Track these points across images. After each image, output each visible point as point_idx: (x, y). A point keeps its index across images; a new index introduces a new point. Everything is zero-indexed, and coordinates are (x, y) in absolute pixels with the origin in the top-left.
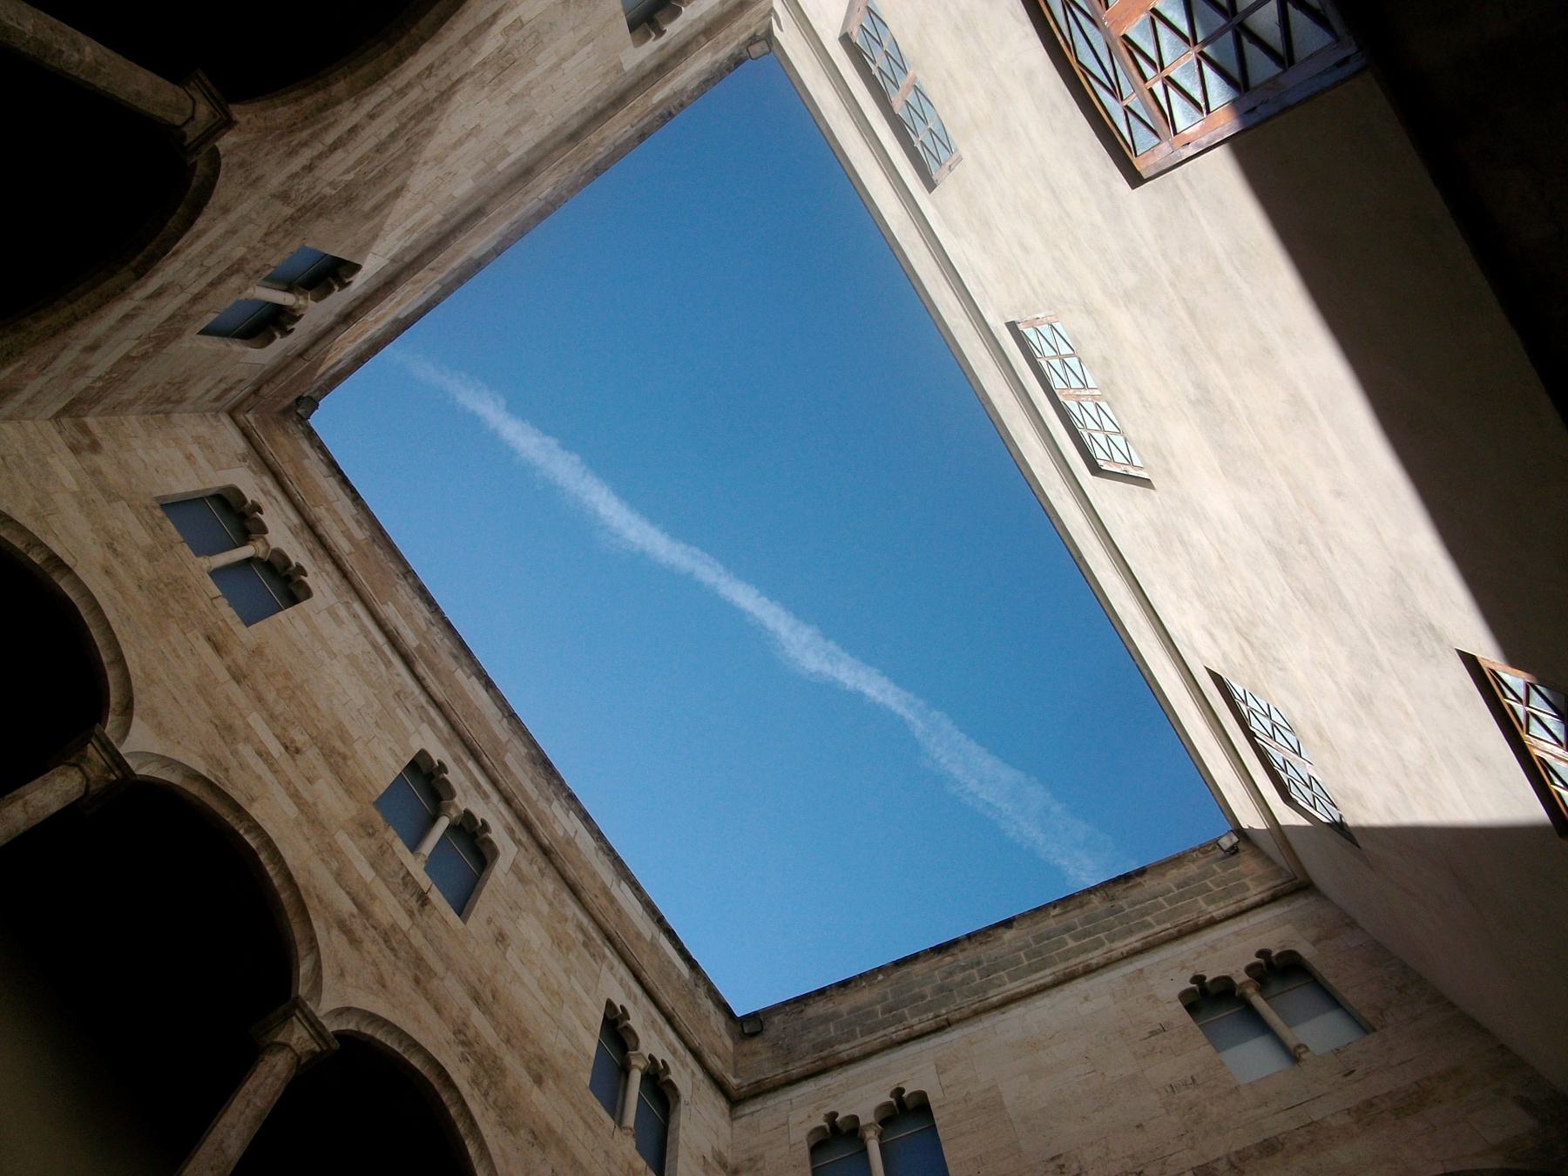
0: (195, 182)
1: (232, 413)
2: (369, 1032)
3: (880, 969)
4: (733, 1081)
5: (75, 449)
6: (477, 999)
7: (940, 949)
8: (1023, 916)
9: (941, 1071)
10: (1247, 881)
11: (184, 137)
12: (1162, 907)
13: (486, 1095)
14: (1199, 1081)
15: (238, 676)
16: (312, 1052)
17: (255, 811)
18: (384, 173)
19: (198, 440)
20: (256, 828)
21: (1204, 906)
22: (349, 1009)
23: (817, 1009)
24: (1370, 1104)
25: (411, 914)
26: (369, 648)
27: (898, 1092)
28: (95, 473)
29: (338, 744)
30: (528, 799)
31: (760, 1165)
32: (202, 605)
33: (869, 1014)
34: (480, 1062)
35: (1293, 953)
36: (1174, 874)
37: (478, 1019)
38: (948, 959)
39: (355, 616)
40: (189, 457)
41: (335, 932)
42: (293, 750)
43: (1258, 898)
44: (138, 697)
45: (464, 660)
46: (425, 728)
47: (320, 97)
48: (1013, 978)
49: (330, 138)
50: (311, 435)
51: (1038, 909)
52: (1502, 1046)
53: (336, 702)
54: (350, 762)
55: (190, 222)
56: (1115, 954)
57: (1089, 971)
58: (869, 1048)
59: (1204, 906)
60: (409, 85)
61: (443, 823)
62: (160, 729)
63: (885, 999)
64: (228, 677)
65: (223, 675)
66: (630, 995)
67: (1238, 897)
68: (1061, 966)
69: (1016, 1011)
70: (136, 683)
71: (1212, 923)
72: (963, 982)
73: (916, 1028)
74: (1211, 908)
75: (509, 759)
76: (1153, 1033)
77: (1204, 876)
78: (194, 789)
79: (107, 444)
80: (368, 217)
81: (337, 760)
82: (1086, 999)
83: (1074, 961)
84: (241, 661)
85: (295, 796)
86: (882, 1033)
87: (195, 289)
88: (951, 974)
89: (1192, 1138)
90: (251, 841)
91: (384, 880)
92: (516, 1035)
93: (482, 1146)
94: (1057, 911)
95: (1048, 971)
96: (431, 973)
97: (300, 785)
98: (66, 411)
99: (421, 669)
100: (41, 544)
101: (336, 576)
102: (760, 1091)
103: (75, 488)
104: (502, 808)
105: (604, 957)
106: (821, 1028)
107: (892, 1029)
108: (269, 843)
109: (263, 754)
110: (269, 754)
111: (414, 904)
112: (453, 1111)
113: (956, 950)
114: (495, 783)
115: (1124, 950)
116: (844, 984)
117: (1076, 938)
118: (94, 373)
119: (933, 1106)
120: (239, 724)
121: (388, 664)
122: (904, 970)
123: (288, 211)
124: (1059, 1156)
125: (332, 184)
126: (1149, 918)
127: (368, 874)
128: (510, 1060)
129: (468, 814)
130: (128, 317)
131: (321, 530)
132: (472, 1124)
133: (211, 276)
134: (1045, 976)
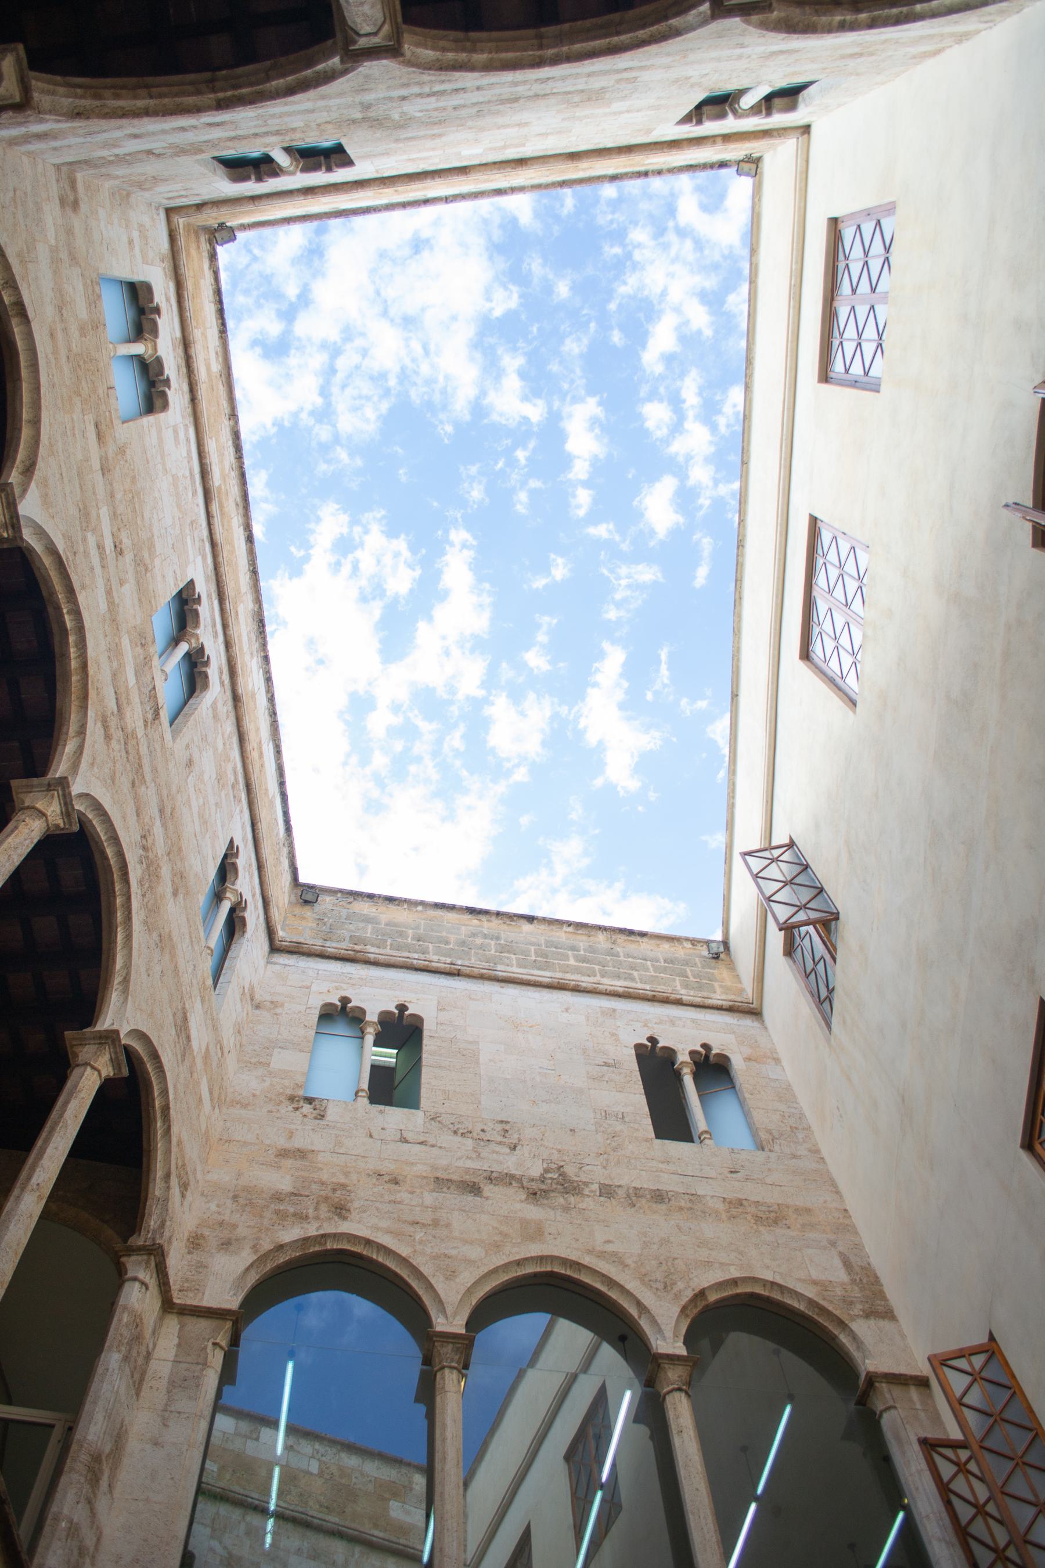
0: (320, 67)
1: (169, 211)
2: (90, 816)
3: (422, 903)
4: (281, 934)
5: (63, 202)
6: (161, 811)
7: (472, 911)
9: (441, 1009)
10: (716, 984)
11: (355, 42)
12: (647, 970)
13: (144, 896)
14: (627, 1119)
15: (105, 470)
16: (57, 826)
17: (81, 598)
18: (440, 122)
19: (141, 227)
20: (77, 613)
21: (679, 988)
22: (87, 795)
23: (363, 908)
24: (740, 1203)
25: (145, 721)
26: (188, 474)
27: (402, 1008)
28: (70, 232)
29: (146, 555)
30: (241, 649)
31: (279, 1011)
32: (100, 391)
33: (401, 934)
34: (148, 867)
35: (726, 1058)
36: (666, 946)
37: (158, 830)
38: (475, 922)
39: (188, 440)
40: (131, 242)
41: (99, 724)
42: (119, 551)
43: (720, 1003)
44: (40, 464)
45: (241, 510)
46: (199, 559)
47: (463, 56)
48: (519, 966)
49: (437, 88)
50: (213, 257)
51: (557, 921)
52: (846, 1210)
53: (155, 516)
54: (148, 574)
55: (291, 91)
57: (576, 989)
58: (393, 960)
59: (679, 988)
60: (525, 82)
61: (184, 648)
62: (46, 501)
63: (417, 927)
64: (98, 467)
65: (96, 465)
66: (244, 839)
67: (705, 994)
68: (559, 975)
69: (512, 991)
70: (42, 451)
71: (679, 1003)
72: (482, 947)
73: (434, 964)
74: (683, 992)
75: (241, 609)
76: (606, 1064)
77: (686, 963)
78: (47, 561)
79: (84, 207)
80: (397, 140)
81: (142, 567)
82: (567, 1010)
83: (568, 976)
84: (110, 454)
85: (109, 592)
87: (240, 133)
88: (474, 935)
89: (607, 1160)
90: (69, 622)
91: (139, 689)
92: (175, 851)
93: (129, 937)
94: (570, 929)
95: (548, 974)
96: (143, 781)
97: (114, 582)
98: (70, 164)
99: (215, 508)
100: (15, 288)
101: (187, 397)
102: (297, 950)
103: (53, 242)
104: (222, 648)
105: (240, 801)
106: (361, 925)
108: (81, 629)
109: (100, 547)
110: (104, 548)
111: (150, 716)
112: (119, 901)
113: (484, 918)
114: (225, 626)
116: (390, 900)
117: (578, 959)
118: (117, 151)
119: (426, 1033)
120: (94, 514)
121: (195, 493)
122: (439, 913)
123: (359, 116)
124: (507, 1122)
125: (403, 114)
126: (635, 974)
127: (132, 681)
128: (165, 872)
129: (201, 650)
130: (183, 129)
131: (192, 352)
132: (128, 918)
133: (264, 130)
134: (545, 975)
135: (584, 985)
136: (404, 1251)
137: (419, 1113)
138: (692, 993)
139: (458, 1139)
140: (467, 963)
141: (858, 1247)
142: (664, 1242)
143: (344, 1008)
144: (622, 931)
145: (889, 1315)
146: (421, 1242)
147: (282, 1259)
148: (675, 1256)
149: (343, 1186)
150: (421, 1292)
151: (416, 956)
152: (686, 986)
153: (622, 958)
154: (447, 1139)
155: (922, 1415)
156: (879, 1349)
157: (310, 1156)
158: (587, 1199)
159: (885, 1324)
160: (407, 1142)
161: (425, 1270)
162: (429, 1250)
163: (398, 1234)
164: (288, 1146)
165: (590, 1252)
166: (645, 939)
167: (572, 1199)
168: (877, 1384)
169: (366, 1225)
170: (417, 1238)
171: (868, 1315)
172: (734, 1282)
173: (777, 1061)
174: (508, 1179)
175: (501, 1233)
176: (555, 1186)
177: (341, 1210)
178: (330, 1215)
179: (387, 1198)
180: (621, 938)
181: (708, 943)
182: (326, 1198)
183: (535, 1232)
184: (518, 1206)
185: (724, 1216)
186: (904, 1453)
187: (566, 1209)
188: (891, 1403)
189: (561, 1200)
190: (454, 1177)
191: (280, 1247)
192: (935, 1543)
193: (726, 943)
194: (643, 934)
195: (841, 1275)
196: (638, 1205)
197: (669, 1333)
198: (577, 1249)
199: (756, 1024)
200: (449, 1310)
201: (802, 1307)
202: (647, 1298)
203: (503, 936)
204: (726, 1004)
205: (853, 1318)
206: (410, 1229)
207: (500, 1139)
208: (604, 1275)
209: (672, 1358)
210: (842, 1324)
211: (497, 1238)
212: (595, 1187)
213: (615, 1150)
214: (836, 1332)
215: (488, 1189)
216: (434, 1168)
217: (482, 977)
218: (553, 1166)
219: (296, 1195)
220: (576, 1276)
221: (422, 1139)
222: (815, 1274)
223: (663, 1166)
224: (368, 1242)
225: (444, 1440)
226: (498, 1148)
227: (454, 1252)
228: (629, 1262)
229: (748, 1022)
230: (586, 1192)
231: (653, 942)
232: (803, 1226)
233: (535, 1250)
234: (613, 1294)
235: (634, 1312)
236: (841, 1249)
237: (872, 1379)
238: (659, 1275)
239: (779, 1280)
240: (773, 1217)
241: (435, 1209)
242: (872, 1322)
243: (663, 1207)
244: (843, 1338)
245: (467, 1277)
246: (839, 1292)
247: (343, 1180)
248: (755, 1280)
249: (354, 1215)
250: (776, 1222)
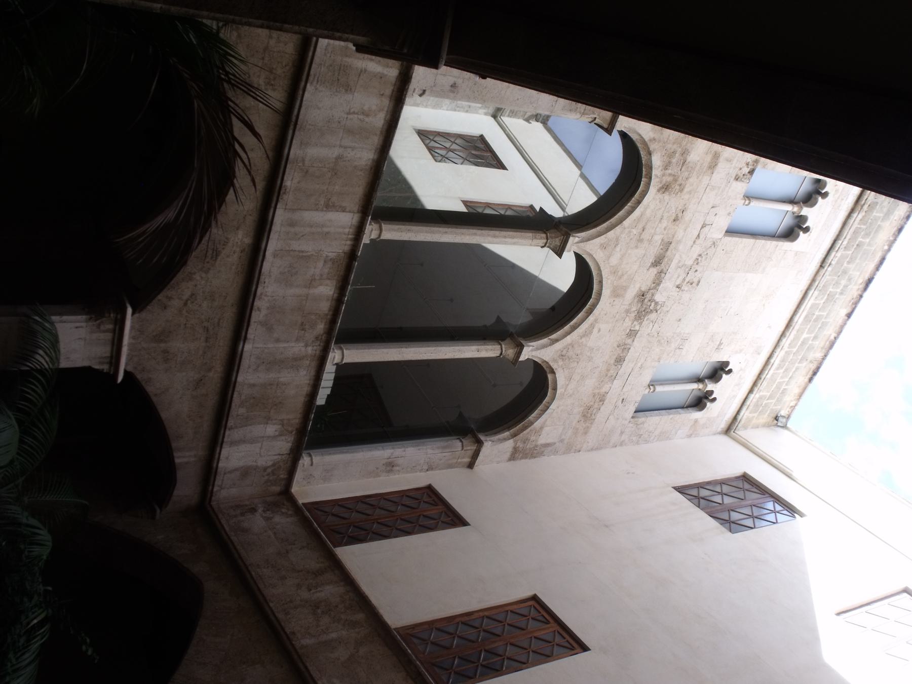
3: (889, 250)
7: (870, 281)
8: (845, 324)
10: (756, 415)
12: (782, 378)
21: (761, 394)
24: (602, 400)
27: (807, 230)
33: (867, 235)
36: (797, 391)
38: (861, 281)
43: (742, 414)
56: (778, 350)
57: (783, 335)
59: (761, 394)
67: (751, 408)
68: (797, 327)
69: (799, 296)
71: (751, 391)
74: (757, 396)
76: (721, 344)
86: (848, 237)
106: (885, 210)
107: (845, 243)
115: (775, 355)
116: (900, 230)
124: (698, 285)
126: (782, 371)
134: (799, 319)
135: (784, 340)
136: (626, 223)
137: (721, 235)
138: (755, 400)
139: (695, 256)
140: (827, 273)
141: (556, 452)
142: (590, 359)
143: (819, 193)
144: (818, 368)
145: (513, 458)
146: (630, 232)
147: (643, 153)
149: (681, 190)
150: (598, 228)
151: (845, 243)
152: (761, 398)
153: (797, 365)
154: (697, 250)
155: (455, 461)
156: (495, 449)
157: (710, 171)
159: (508, 455)
160: (702, 227)
161: (611, 234)
162: (623, 236)
163: (639, 219)
164: (721, 159)
165: (596, 321)
166: (807, 380)
167: (633, 315)
169: (651, 203)
171: (516, 450)
172: (555, 389)
173: (690, 436)
174: (657, 282)
175: (623, 275)
176: (645, 305)
177: (665, 188)
178: (664, 182)
179: (666, 215)
180: (813, 367)
181: (788, 417)
182: (676, 180)
183: (617, 293)
184: (638, 286)
185: (597, 391)
186: (438, 448)
187: (627, 311)
190: (669, 253)
191: (650, 154)
192: (392, 451)
193: (785, 427)
194: (811, 380)
195: (542, 440)
197: (534, 353)
199: (719, 430)
200: (582, 245)
201: (531, 418)
202: (558, 346)
203: (842, 297)
204: (739, 417)
205: (516, 442)
206: (640, 226)
207: (687, 280)
209: (519, 354)
210: (514, 435)
211: (620, 273)
212: (637, 328)
213: (659, 341)
215: (654, 271)
216: (679, 242)
217: (813, 280)
218: (658, 307)
219: (684, 163)
221: (701, 236)
223: (639, 365)
224: (639, 202)
225: (505, 237)
226: (681, 278)
227: (618, 249)
228: (583, 339)
229: (723, 425)
230: (636, 323)
231: (803, 384)
232: (577, 429)
233: (606, 292)
234: (567, 328)
235: (554, 336)
236: (557, 444)
237: (480, 443)
238: (571, 353)
239: (549, 411)
240: (588, 415)
241: (650, 241)
242: (511, 449)
243: (612, 361)
244: (507, 434)
245: (599, 255)
246: (533, 438)
247: (686, 190)
248: (553, 399)
249: (660, 196)
250: (584, 416)
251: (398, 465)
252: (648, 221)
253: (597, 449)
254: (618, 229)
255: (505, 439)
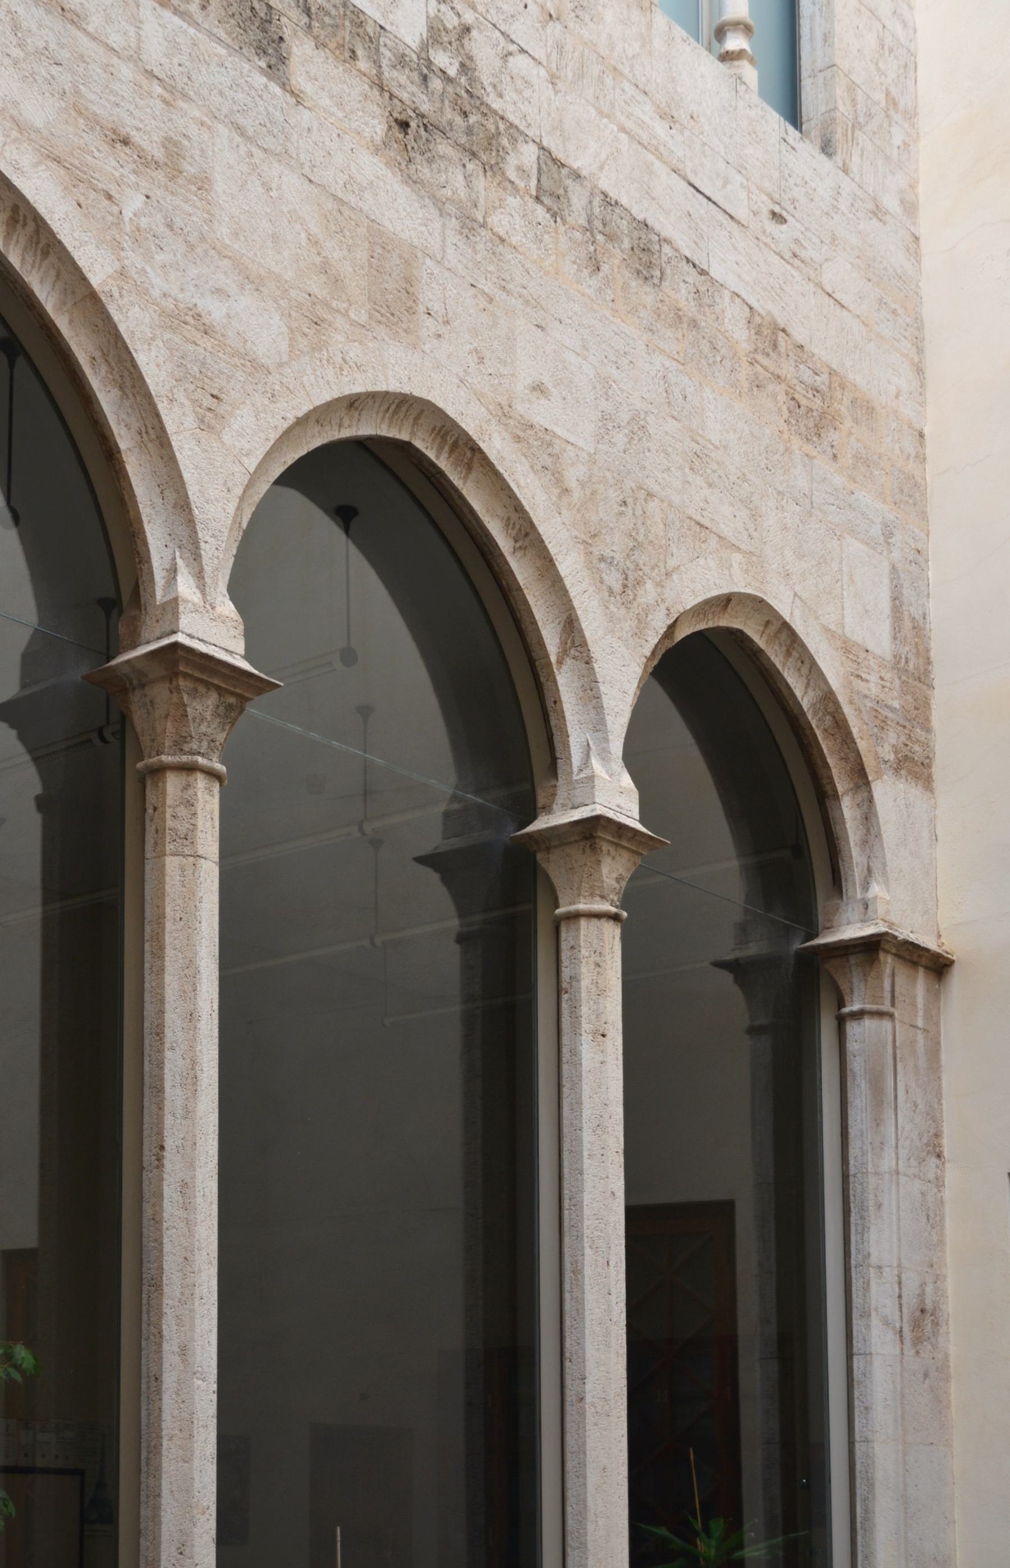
136: (99, 271)
146: (138, 236)
148: (655, 488)
150: (124, 439)
155: (920, 1037)
158: (513, 201)
159: (914, 792)
161: (153, 365)
162: (158, 283)
163: (77, 178)
168: (882, 956)
170: (128, 214)
175: (325, 268)
185: (745, 371)
186: (878, 1122)
187: (470, 225)
188: (886, 1007)
189: (458, 179)
196: (605, 268)
198: (479, 397)
201: (805, 698)
206: (108, 164)
208: (519, 508)
211: (317, 286)
212: (528, 155)
214: (840, 789)
220: (455, 478)
222: (857, 631)
227: (215, 310)
228: (572, 476)
234: (521, 570)
243: (647, 296)
244: (848, 809)
251: (922, 1295)
252: (77, 109)
253: (919, 345)
254: (131, 320)
255: (868, 816)
